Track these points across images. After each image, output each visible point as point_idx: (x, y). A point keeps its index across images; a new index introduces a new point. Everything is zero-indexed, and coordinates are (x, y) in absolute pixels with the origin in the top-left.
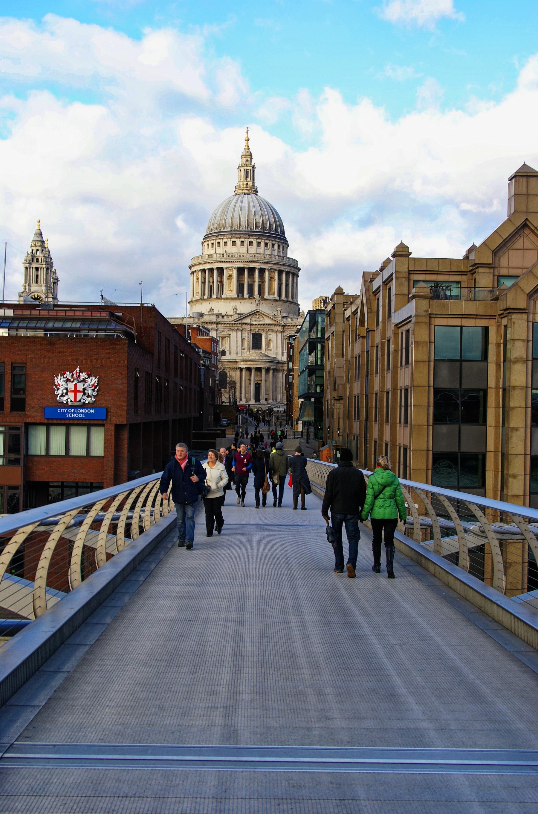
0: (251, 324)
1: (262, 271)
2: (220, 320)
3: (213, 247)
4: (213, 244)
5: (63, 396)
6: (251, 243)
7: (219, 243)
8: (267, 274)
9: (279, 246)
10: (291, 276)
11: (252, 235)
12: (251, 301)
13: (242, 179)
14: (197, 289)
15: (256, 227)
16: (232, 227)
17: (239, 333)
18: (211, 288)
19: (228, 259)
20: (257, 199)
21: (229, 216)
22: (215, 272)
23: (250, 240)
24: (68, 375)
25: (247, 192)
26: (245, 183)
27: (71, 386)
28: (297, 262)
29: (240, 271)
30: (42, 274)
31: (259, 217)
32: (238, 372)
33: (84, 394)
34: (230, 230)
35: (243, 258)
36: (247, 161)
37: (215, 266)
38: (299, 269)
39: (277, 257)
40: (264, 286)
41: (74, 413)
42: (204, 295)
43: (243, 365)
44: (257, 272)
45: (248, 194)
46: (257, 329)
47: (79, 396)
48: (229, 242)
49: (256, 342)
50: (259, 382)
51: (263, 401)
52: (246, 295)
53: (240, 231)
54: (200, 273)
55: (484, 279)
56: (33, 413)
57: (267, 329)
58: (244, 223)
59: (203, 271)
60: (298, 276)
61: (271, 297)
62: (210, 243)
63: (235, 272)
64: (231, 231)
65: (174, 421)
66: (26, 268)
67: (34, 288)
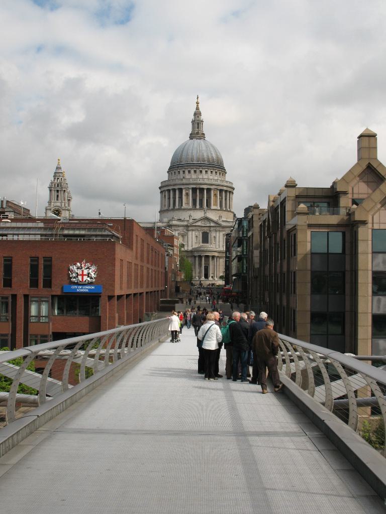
0: (201, 226)
1: (209, 190)
3: (175, 174)
4: (175, 172)
5: (75, 278)
6: (201, 172)
9: (220, 173)
10: (228, 194)
12: (201, 211)
14: (165, 202)
17: (194, 232)
22: (177, 192)
24: (79, 264)
27: (80, 272)
28: (232, 183)
29: (194, 190)
30: (61, 194)
32: (193, 259)
33: (88, 277)
35: (195, 182)
38: (234, 189)
40: (210, 200)
41: (82, 288)
42: (169, 206)
43: (196, 254)
44: (205, 191)
46: (206, 229)
47: (85, 278)
48: (187, 172)
49: (205, 238)
50: (207, 265)
51: (210, 278)
52: (198, 207)
54: (167, 192)
55: (345, 202)
57: (212, 229)
58: (195, 158)
59: (169, 191)
60: (233, 193)
63: (191, 191)
64: (187, 164)
65: (147, 293)
66: (51, 191)
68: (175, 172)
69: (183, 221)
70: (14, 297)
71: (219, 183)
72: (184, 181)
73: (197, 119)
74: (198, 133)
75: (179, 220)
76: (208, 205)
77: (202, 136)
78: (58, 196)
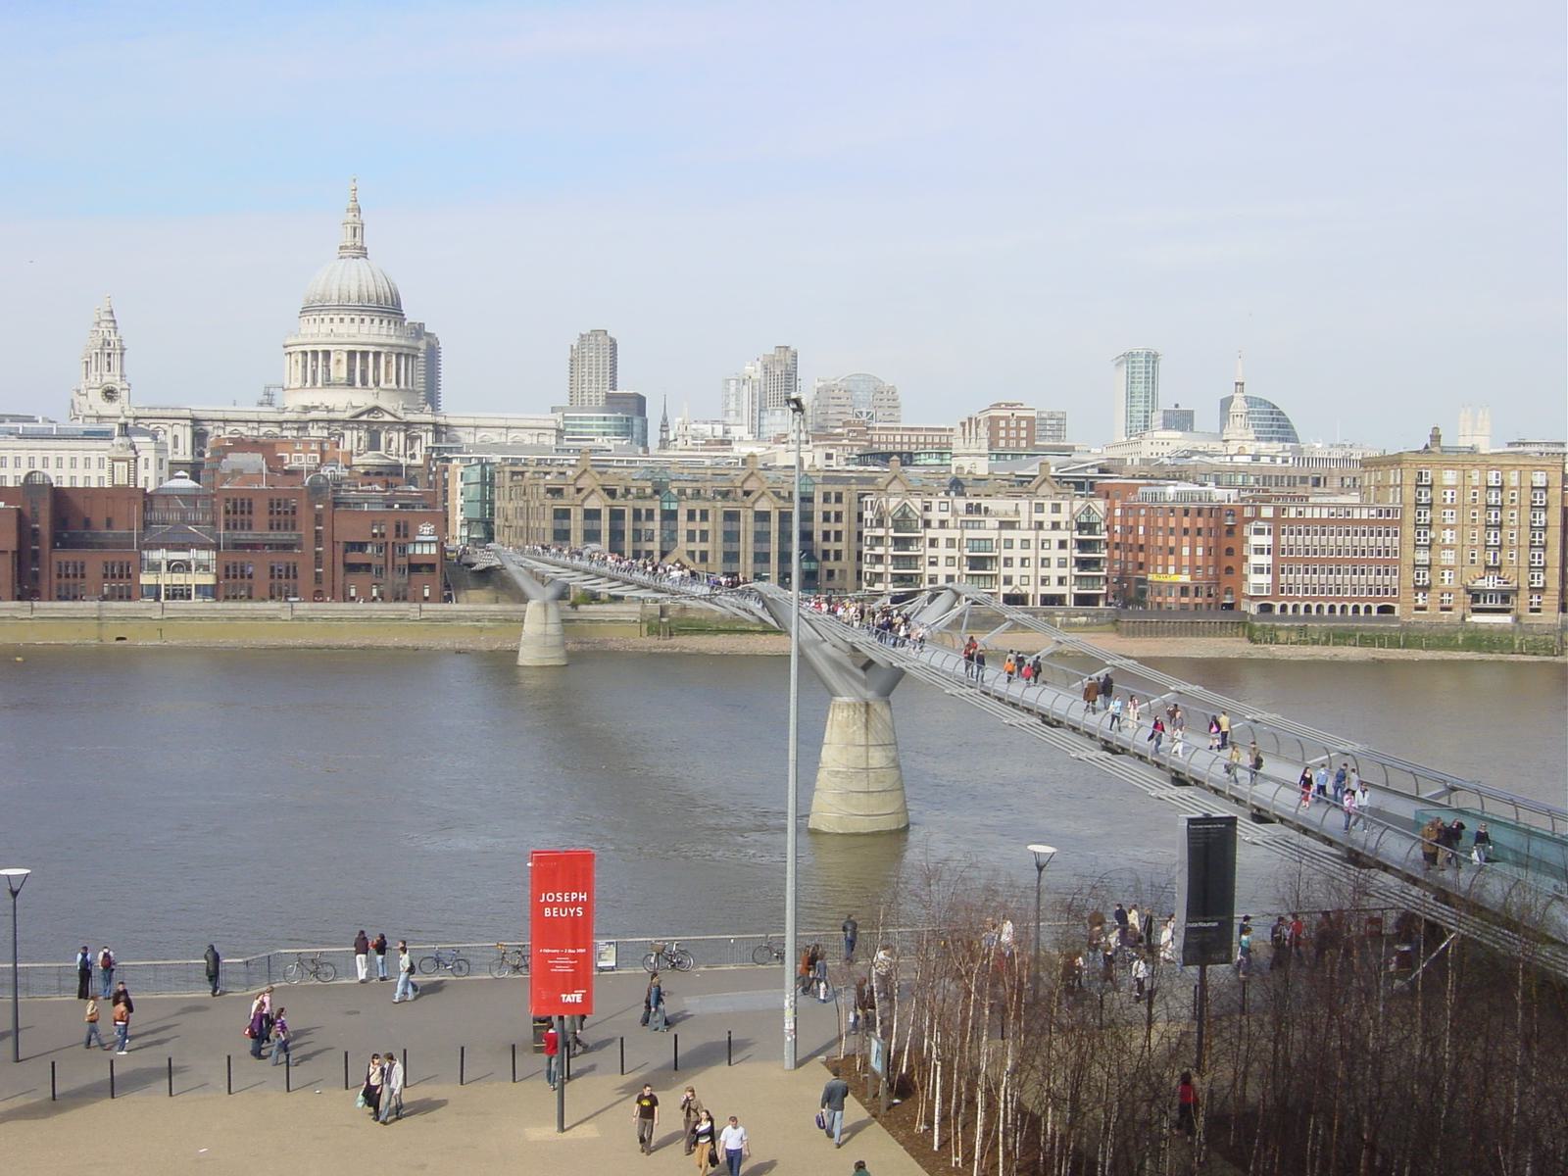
2: (332, 416)
6: (363, 320)
8: (383, 357)
15: (369, 301)
17: (355, 432)
18: (314, 373)
19: (337, 340)
21: (335, 288)
22: (320, 355)
29: (351, 354)
30: (116, 361)
31: (372, 289)
37: (320, 348)
46: (375, 428)
48: (337, 319)
49: (374, 445)
52: (358, 384)
54: (300, 355)
56: (411, 539)
58: (354, 296)
59: (305, 353)
61: (388, 386)
62: (311, 319)
63: (345, 355)
67: (106, 379)
69: (333, 410)
70: (387, 543)
71: (393, 341)
72: (332, 339)
73: (356, 219)
74: (355, 247)
75: (329, 410)
76: (377, 383)
77: (362, 252)
78: (109, 364)
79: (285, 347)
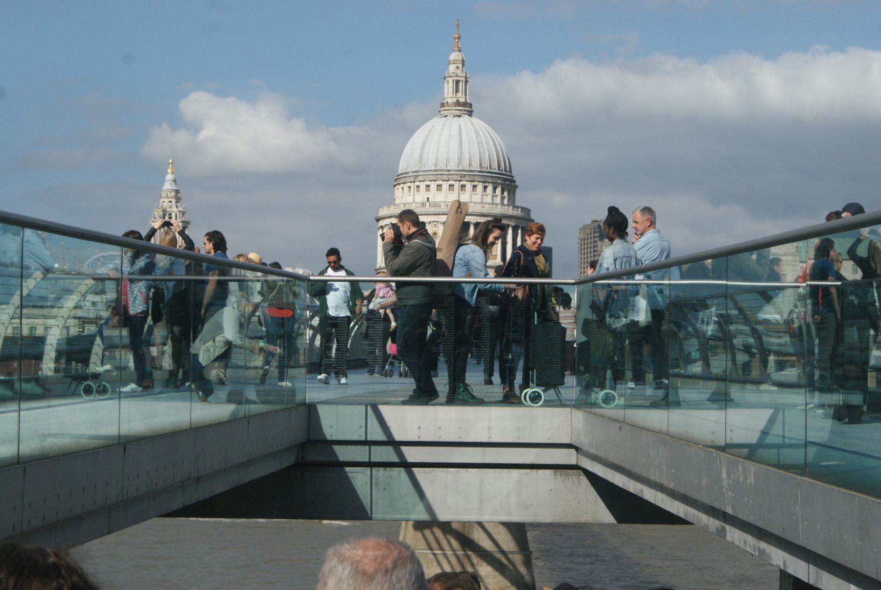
3: (410, 191)
4: (410, 187)
7: (418, 187)
10: (520, 232)
11: (465, 175)
13: (450, 95)
16: (436, 165)
19: (432, 210)
20: (472, 123)
23: (462, 183)
25: (457, 113)
26: (455, 100)
28: (529, 211)
34: (433, 168)
36: (458, 68)
39: (500, 206)
45: (459, 116)
48: (433, 186)
53: (449, 171)
62: (406, 186)
64: (436, 171)
68: (410, 187)
73: (459, 72)
79: (378, 220)
